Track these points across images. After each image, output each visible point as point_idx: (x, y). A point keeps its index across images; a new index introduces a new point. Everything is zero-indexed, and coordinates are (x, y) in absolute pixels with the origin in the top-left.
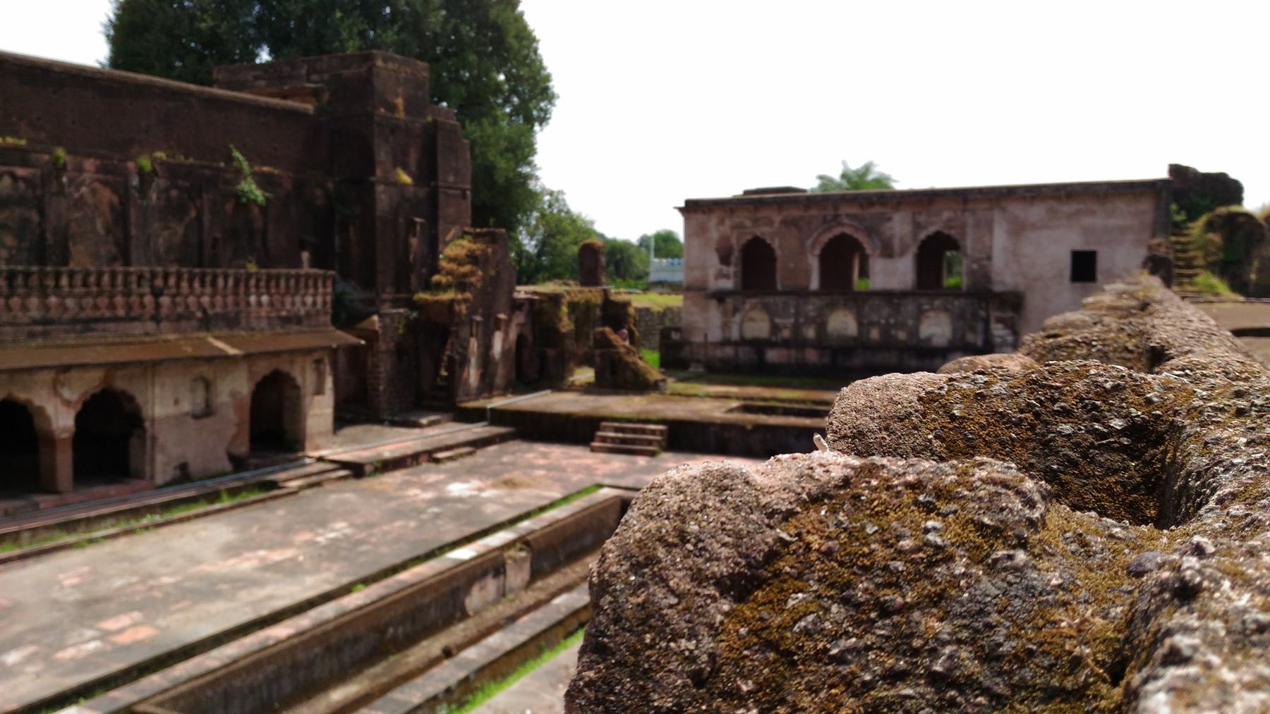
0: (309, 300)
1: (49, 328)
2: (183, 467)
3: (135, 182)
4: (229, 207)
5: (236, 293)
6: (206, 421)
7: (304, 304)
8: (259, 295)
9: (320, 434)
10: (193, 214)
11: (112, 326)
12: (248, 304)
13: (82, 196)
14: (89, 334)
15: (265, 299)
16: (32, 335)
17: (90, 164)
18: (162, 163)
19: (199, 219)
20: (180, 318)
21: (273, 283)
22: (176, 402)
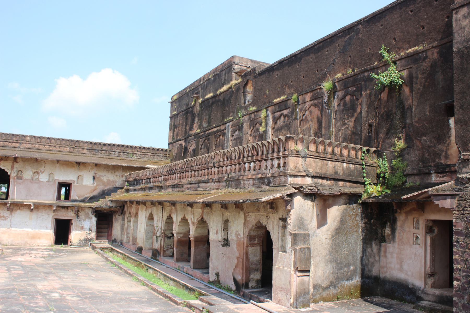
0: (276, 162)
1: (191, 186)
2: (217, 274)
3: (326, 100)
4: (384, 96)
5: (240, 164)
6: (225, 248)
7: (272, 165)
8: (250, 163)
9: (282, 289)
10: (359, 110)
11: (203, 185)
12: (245, 167)
13: (306, 117)
14: (198, 189)
15: (252, 164)
16: (189, 189)
17: (308, 97)
18: (340, 80)
19: (361, 111)
20: (219, 181)
21: (255, 154)
22: (217, 233)
